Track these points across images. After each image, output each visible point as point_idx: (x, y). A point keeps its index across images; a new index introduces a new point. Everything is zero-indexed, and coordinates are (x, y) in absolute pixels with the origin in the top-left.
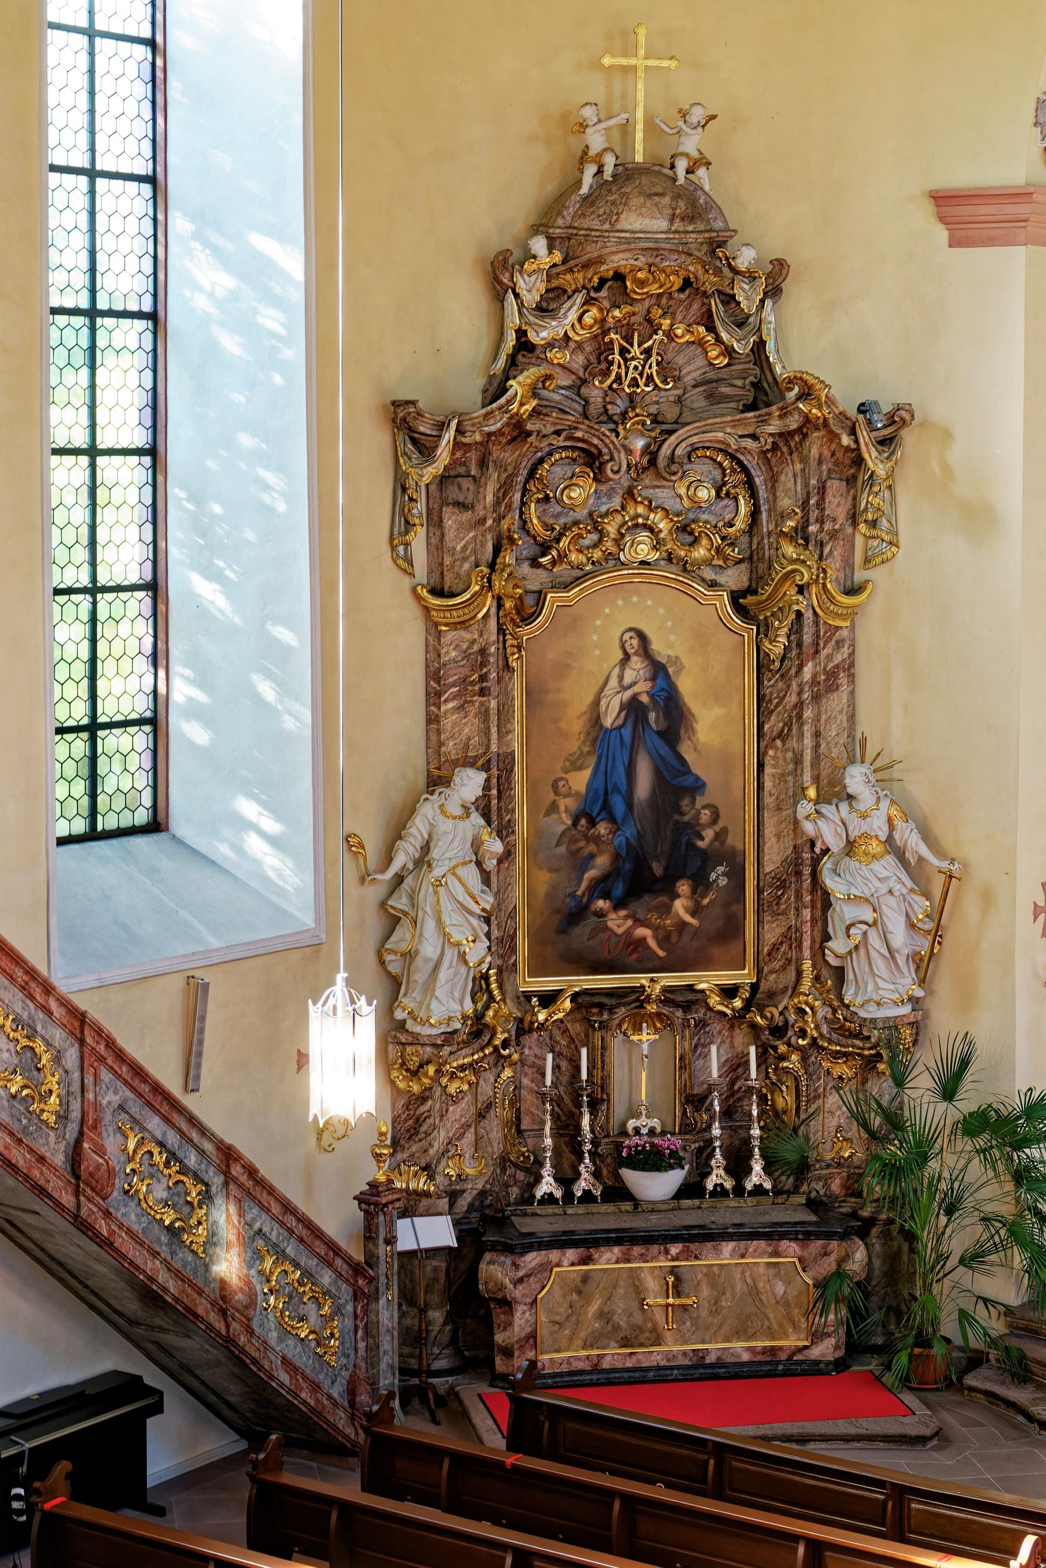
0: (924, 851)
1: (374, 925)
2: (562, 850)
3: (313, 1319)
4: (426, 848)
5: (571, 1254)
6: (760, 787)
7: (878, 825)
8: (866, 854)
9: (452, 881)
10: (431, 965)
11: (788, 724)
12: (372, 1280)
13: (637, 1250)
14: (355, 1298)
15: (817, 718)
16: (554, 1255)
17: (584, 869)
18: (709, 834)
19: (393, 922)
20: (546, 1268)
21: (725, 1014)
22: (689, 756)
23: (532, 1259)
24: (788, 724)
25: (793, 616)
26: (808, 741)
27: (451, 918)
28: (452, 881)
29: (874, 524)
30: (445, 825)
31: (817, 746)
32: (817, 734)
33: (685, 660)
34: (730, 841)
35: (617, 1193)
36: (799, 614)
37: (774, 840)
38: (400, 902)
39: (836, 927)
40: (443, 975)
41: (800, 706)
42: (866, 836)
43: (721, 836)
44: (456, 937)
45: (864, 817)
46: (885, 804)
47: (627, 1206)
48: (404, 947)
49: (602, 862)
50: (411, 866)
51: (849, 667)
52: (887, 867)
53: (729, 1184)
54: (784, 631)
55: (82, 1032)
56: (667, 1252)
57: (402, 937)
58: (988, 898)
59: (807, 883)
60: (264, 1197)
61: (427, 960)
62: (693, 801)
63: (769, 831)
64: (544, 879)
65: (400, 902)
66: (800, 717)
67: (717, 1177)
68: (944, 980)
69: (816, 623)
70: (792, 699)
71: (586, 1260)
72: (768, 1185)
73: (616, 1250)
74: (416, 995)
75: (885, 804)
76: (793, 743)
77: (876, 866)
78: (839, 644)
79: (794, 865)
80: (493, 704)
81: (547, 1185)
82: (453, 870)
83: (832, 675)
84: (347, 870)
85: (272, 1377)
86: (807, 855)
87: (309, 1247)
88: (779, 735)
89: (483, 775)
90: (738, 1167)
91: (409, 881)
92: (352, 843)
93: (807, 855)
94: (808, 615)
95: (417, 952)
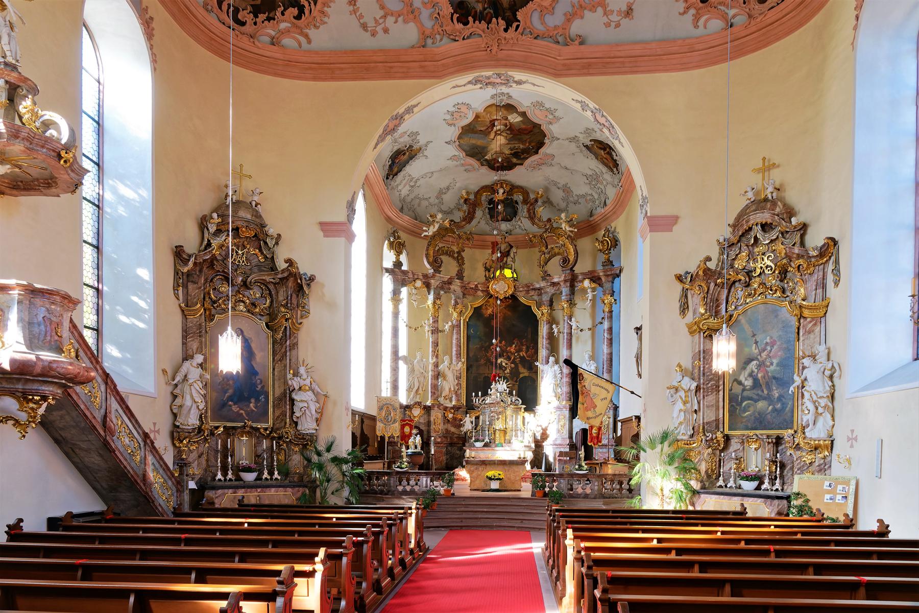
0: (319, 391)
1: (169, 398)
2: (220, 387)
3: (166, 494)
4: (186, 376)
5: (231, 491)
6: (273, 375)
7: (308, 382)
8: (305, 389)
9: (195, 384)
10: (188, 409)
11: (283, 357)
12: (182, 486)
13: (249, 490)
14: (177, 492)
15: (290, 355)
16: (226, 491)
17: (226, 393)
18: (260, 387)
19: (175, 397)
20: (224, 494)
21: (264, 435)
22: (255, 366)
23: (220, 492)
24: (283, 357)
25: (284, 328)
26: (288, 361)
27: (195, 394)
28: (195, 384)
29: (304, 307)
30: (192, 369)
31: (290, 363)
32: (290, 360)
33: (253, 339)
34: (265, 389)
35: (239, 479)
36: (286, 327)
37: (278, 388)
38: (177, 391)
39: (296, 409)
40: (192, 411)
41: (286, 352)
42: (304, 385)
43: (262, 387)
44: (196, 400)
45: (304, 380)
46: (309, 377)
47: (241, 482)
48: (179, 404)
49: (230, 392)
50: (181, 381)
51: (296, 344)
52: (310, 393)
53: (269, 477)
54: (281, 332)
55: (107, 380)
56: (257, 491)
57: (178, 401)
58: (335, 403)
59: (288, 399)
60: (155, 453)
61: (188, 406)
62: (255, 377)
63: (276, 386)
64: (215, 394)
65: (177, 391)
66: (286, 355)
67: (266, 475)
68: (323, 424)
69: (290, 331)
70: (283, 350)
71: (235, 493)
72: (279, 478)
73: (243, 490)
74: (183, 418)
75: (309, 377)
76: (283, 362)
77: (308, 392)
78: (295, 337)
79: (284, 394)
80: (203, 340)
81: (219, 476)
82: (195, 382)
83: (294, 345)
84: (162, 380)
85: (157, 508)
86: (288, 391)
87: (165, 472)
88: (280, 360)
89: (203, 357)
90: (271, 473)
91: (179, 386)
92: (164, 371)
93: (288, 391)
94: (288, 328)
95: (184, 404)
